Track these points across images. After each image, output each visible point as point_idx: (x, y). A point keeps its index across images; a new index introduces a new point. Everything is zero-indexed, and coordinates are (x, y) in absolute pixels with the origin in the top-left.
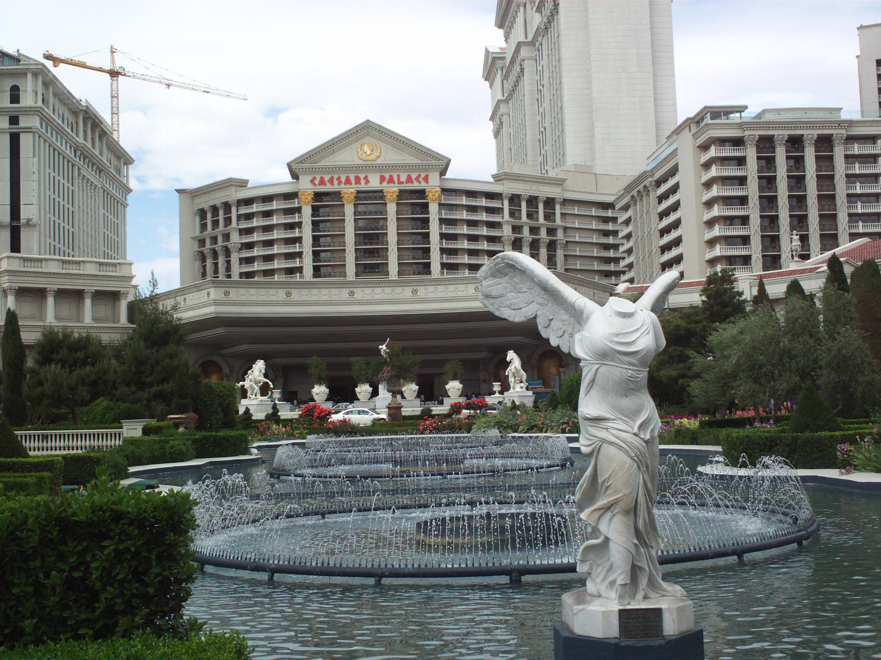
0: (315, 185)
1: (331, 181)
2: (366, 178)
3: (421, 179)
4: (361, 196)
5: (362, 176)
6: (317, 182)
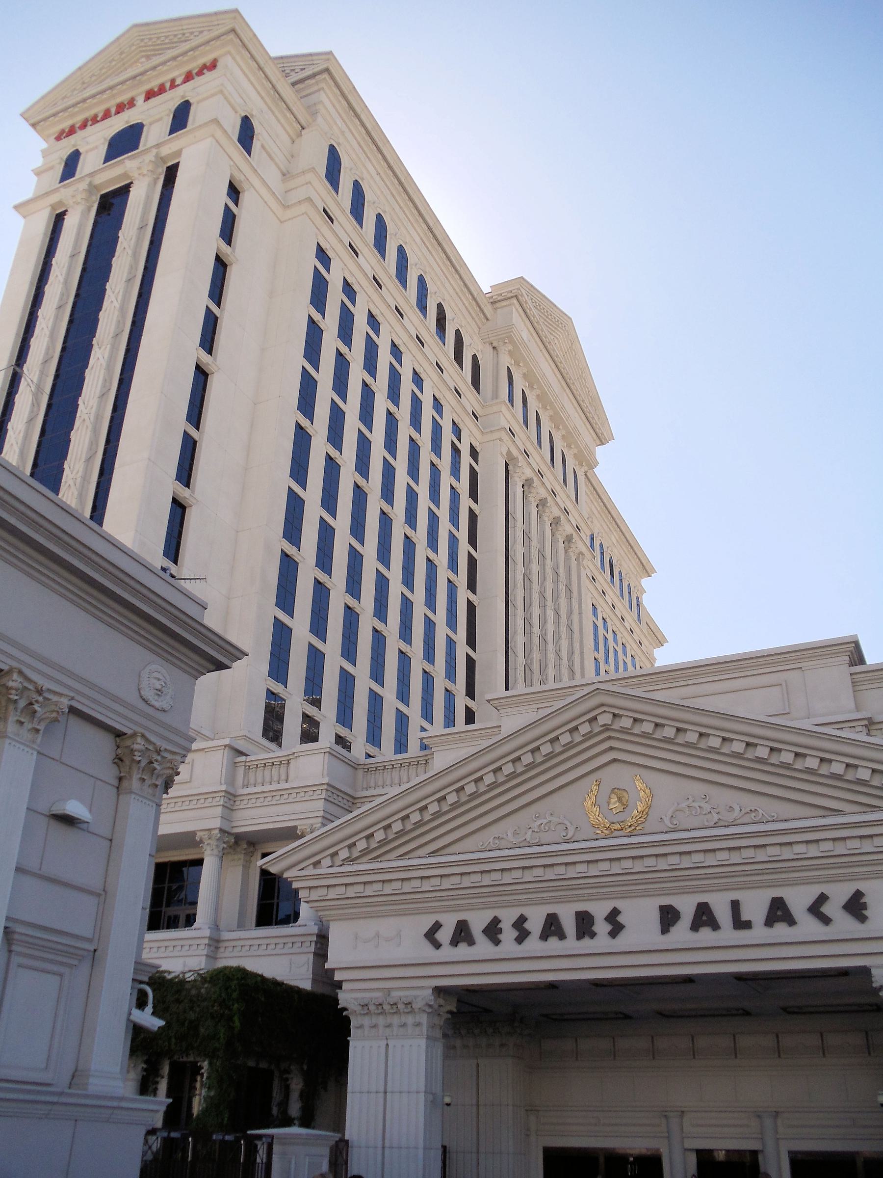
0: (437, 945)
1: (493, 931)
2: (613, 917)
3: (831, 909)
5: (599, 910)
6: (445, 935)
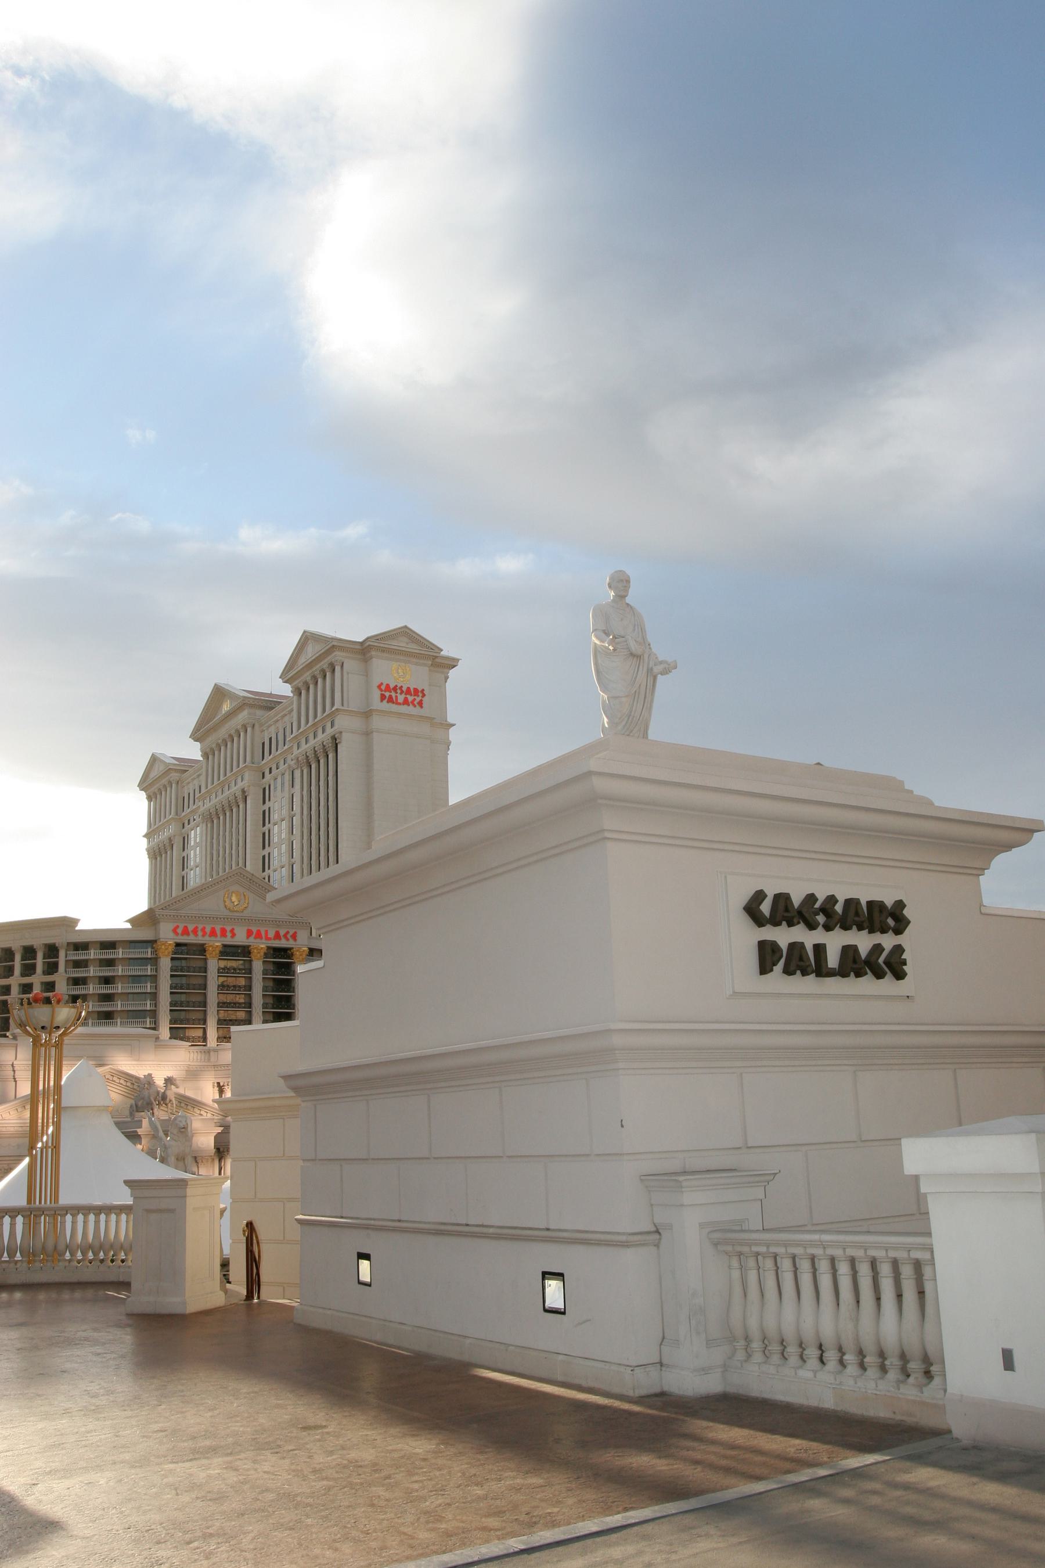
1: (195, 931)
2: (232, 931)
3: (289, 936)
4: (229, 951)
5: (228, 928)
6: (180, 931)
